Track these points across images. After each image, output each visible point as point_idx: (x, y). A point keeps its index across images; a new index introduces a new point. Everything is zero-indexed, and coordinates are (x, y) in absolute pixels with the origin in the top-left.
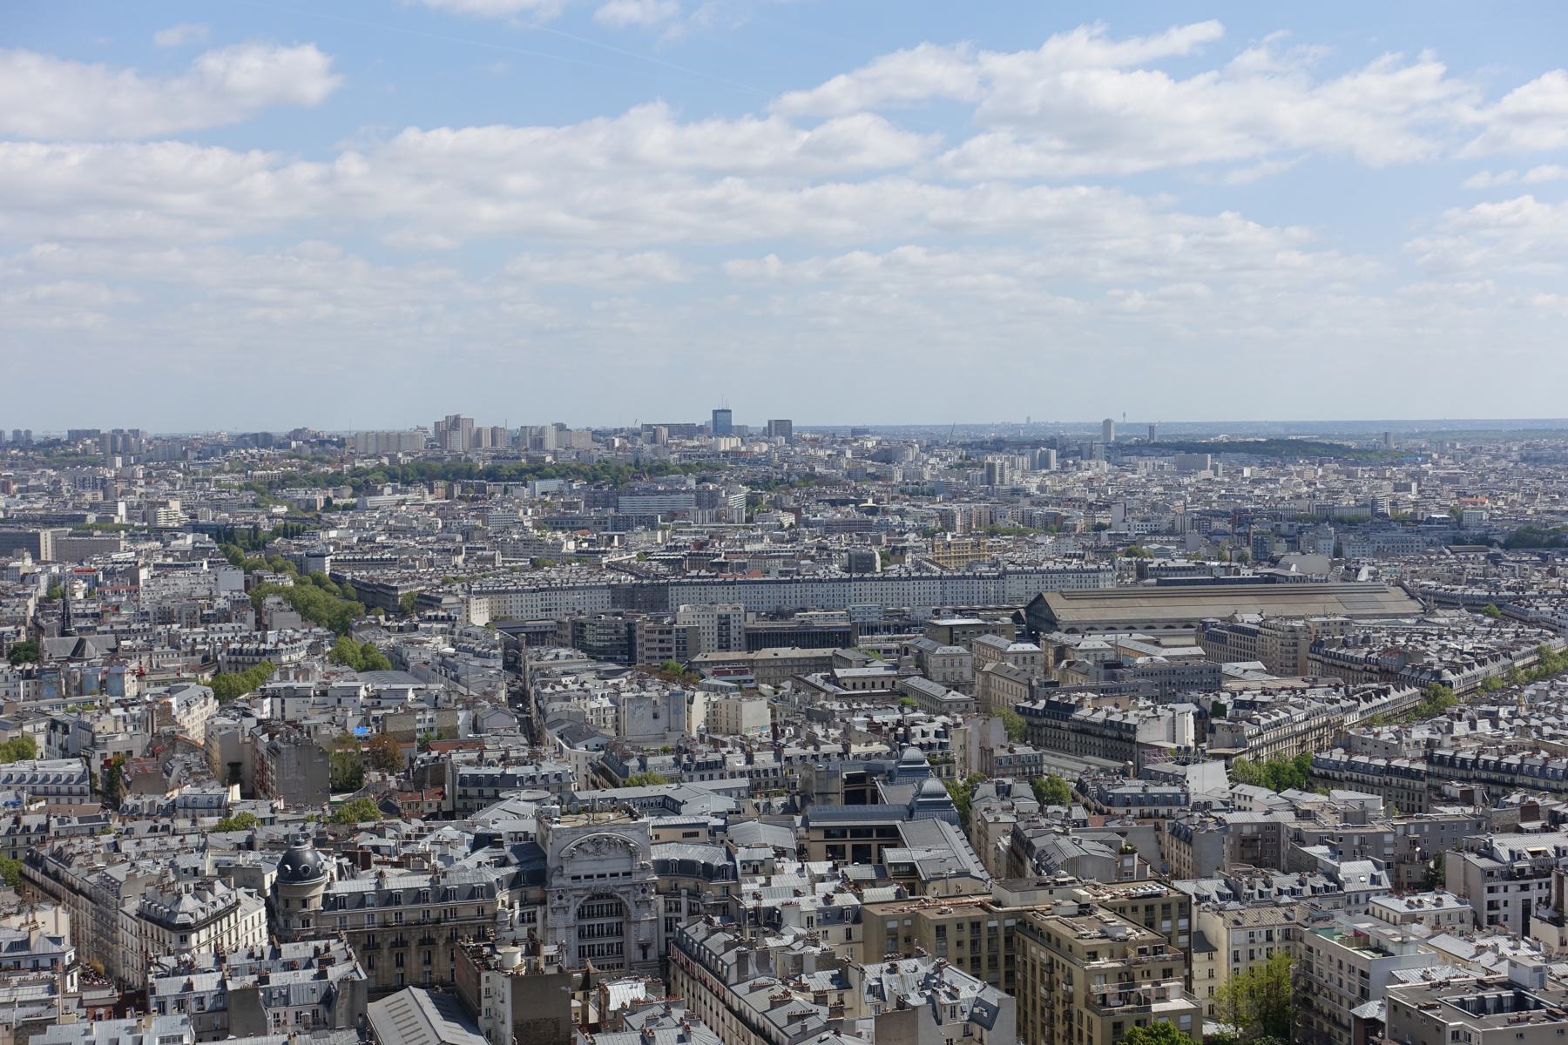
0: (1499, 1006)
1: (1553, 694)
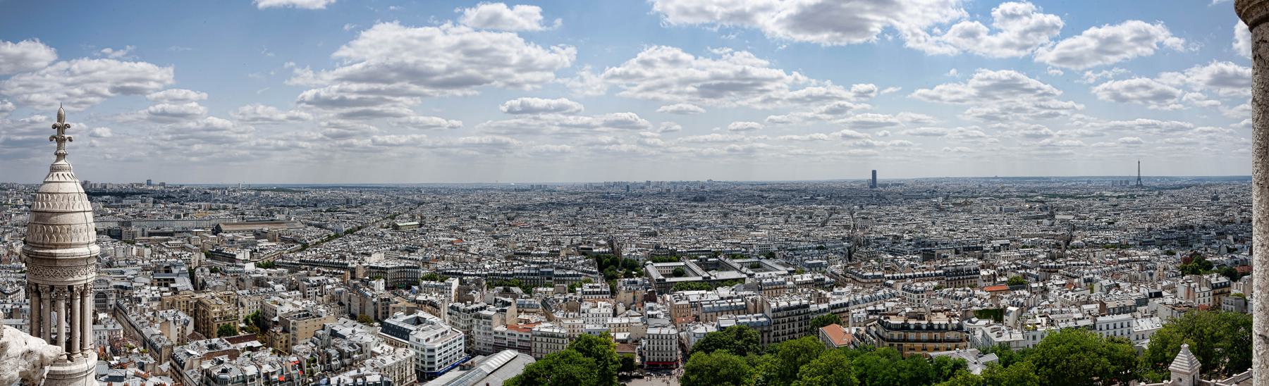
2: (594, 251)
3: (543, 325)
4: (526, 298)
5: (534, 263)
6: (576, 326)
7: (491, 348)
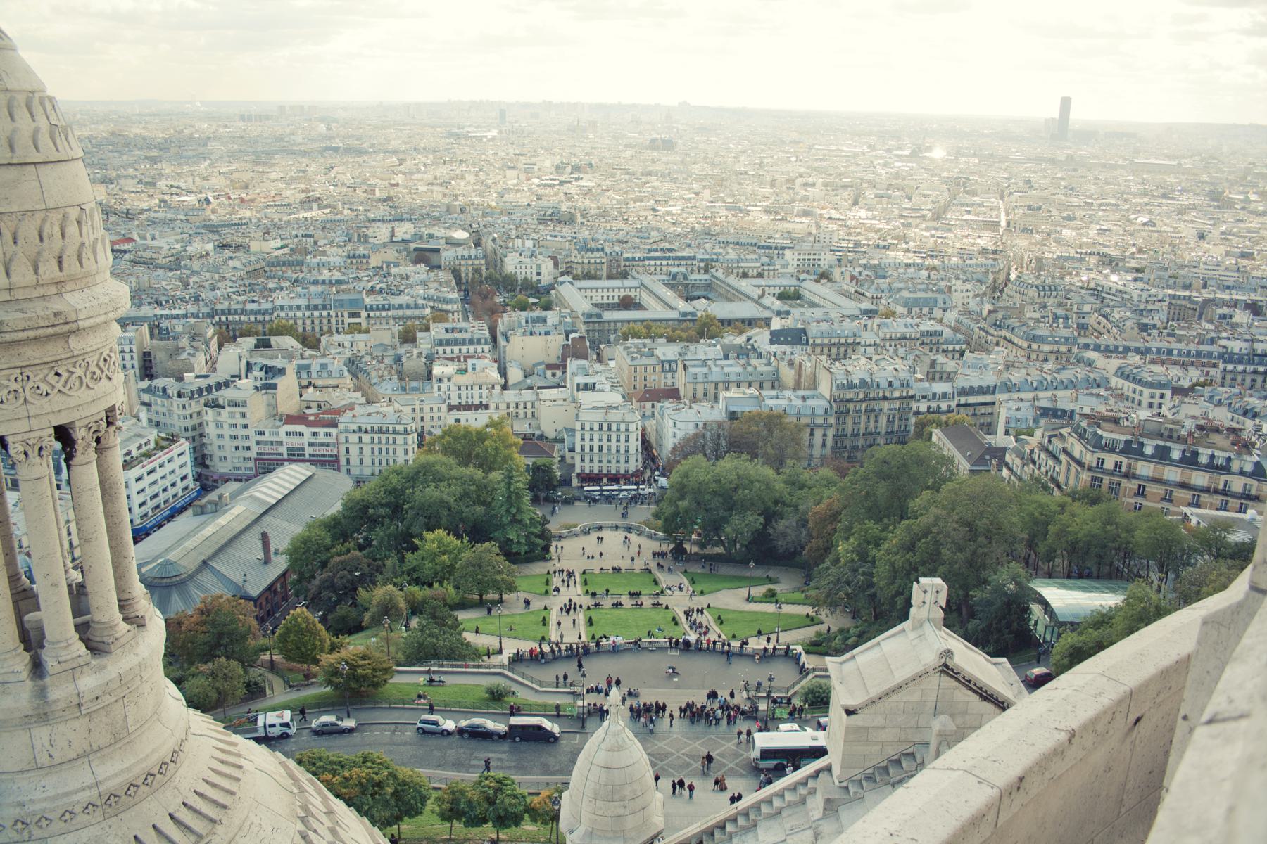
5: (315, 282)
7: (251, 464)
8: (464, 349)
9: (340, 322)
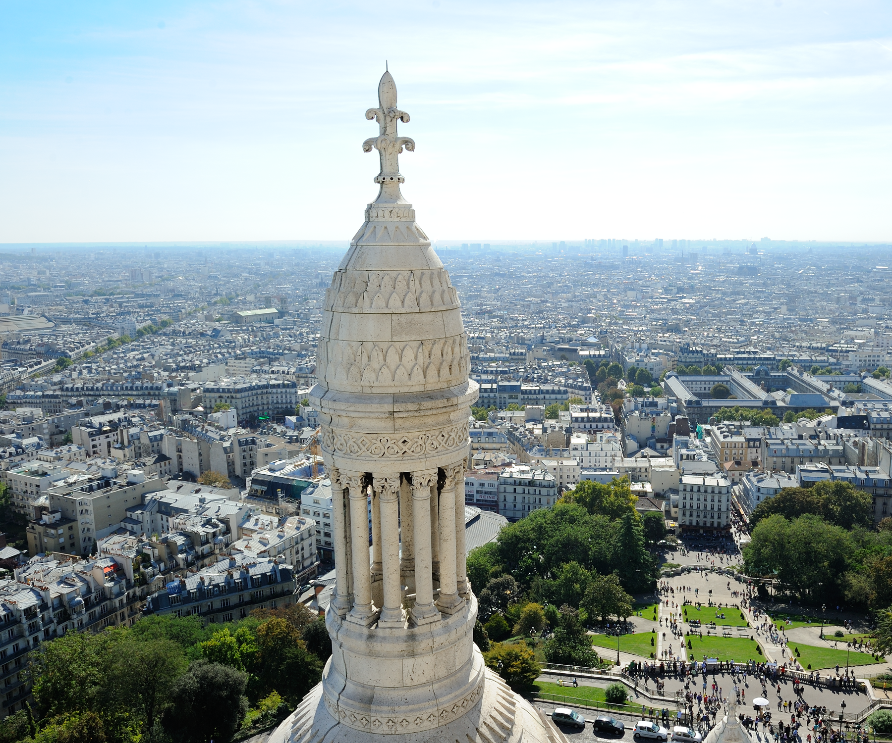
0: (99, 487)
1: (115, 356)
2: (581, 353)
3: (515, 469)
4: (481, 427)
5: (486, 372)
6: (565, 470)
8: (594, 425)
9: (503, 402)
